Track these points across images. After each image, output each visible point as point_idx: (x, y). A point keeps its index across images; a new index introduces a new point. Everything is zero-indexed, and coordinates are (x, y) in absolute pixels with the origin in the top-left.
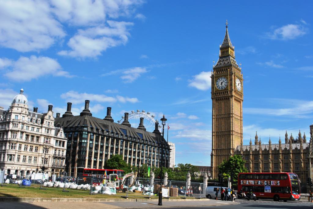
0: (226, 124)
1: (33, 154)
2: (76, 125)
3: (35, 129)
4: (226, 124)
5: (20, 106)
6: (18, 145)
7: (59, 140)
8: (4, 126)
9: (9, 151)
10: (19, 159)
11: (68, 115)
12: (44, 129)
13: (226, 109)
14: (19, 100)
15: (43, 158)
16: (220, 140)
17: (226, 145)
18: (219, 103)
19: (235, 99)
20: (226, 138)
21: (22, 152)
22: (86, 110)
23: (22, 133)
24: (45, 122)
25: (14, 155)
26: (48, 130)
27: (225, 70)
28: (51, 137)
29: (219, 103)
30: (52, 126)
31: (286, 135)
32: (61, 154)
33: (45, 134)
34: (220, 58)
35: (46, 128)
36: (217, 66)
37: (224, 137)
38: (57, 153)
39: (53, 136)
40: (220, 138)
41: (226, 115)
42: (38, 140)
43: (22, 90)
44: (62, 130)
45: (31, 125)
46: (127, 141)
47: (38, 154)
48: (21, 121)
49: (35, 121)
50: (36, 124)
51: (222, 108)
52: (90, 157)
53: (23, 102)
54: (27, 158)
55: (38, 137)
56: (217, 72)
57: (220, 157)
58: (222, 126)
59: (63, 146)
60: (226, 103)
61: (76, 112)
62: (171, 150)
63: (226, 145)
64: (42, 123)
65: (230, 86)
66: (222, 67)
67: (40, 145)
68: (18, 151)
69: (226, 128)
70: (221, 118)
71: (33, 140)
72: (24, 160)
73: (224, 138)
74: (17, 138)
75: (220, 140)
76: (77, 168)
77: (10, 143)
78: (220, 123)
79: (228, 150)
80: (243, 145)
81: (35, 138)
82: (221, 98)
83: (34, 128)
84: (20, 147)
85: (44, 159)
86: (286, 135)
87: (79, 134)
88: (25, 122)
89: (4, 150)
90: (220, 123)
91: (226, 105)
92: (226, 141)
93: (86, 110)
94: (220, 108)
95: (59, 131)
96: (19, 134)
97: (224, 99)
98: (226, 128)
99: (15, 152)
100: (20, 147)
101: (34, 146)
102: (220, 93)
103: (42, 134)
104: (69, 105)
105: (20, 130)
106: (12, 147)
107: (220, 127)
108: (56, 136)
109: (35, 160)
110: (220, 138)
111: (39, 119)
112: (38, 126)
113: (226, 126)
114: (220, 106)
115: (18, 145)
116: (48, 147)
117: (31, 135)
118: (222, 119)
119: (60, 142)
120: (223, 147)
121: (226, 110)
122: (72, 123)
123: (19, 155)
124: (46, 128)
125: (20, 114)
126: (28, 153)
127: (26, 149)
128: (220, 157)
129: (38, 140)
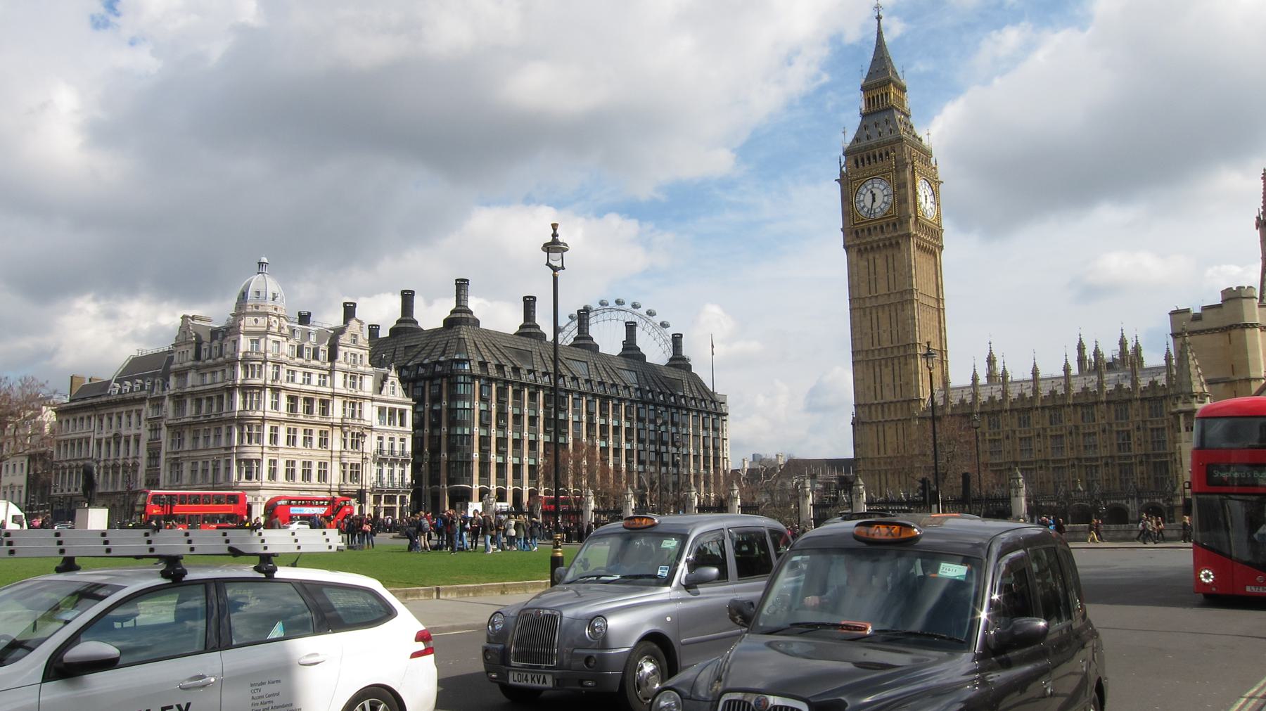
0: (894, 325)
3: (315, 379)
4: (894, 325)
5: (260, 310)
7: (388, 405)
8: (219, 374)
11: (406, 327)
13: (891, 277)
16: (878, 374)
17: (898, 389)
19: (918, 246)
20: (897, 368)
21: (281, 451)
23: (276, 391)
25: (258, 461)
26: (353, 377)
27: (881, 155)
28: (364, 398)
30: (365, 366)
31: (1081, 348)
32: (397, 448)
34: (864, 116)
35: (345, 372)
38: (386, 447)
40: (877, 369)
42: (324, 412)
43: (265, 260)
44: (393, 376)
46: (604, 400)
52: (484, 453)
53: (270, 296)
55: (325, 403)
56: (856, 162)
57: (880, 428)
59: (402, 424)
60: (890, 260)
61: (431, 316)
62: (726, 414)
63: (898, 389)
65: (900, 203)
67: (332, 425)
69: (895, 337)
70: (877, 307)
75: (878, 374)
77: (241, 426)
78: (875, 321)
79: (905, 405)
80: (951, 385)
83: (309, 374)
84: (274, 438)
85: (348, 469)
86: (1081, 348)
87: (445, 385)
88: (284, 358)
89: (226, 449)
90: (875, 321)
91: (891, 265)
92: (897, 379)
94: (872, 277)
95: (385, 377)
97: (885, 245)
98: (895, 337)
100: (274, 438)
101: (316, 430)
102: (869, 230)
104: (407, 298)
106: (250, 436)
107: (876, 335)
108: (376, 396)
109: (323, 475)
110: (877, 369)
113: (894, 332)
115: (267, 427)
117: (302, 396)
119: (392, 411)
120: (889, 396)
123: (275, 461)
124: (345, 372)
126: (300, 453)
127: (291, 440)
128: (880, 428)
129: (324, 412)
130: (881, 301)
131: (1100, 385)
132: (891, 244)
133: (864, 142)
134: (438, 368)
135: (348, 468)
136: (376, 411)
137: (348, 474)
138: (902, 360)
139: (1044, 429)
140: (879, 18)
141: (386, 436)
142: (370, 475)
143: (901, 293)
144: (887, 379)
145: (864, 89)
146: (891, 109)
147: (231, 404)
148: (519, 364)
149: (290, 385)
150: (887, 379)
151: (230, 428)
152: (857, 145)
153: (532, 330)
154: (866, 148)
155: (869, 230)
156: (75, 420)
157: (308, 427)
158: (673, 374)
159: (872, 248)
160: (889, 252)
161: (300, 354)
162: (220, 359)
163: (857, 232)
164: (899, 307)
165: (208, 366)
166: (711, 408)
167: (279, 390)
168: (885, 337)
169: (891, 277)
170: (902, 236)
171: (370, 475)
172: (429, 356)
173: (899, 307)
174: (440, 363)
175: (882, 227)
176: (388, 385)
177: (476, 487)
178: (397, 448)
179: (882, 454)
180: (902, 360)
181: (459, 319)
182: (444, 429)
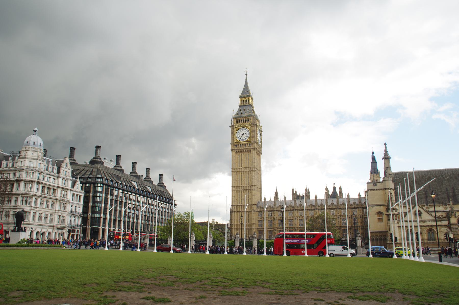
0: (247, 178)
1: (49, 211)
2: (87, 175)
3: (52, 180)
4: (247, 178)
10: (34, 216)
12: (60, 180)
13: (247, 162)
14: (34, 143)
21: (38, 209)
22: (96, 157)
23: (39, 183)
24: (62, 171)
27: (246, 120)
28: (68, 189)
33: (62, 186)
34: (240, 106)
35: (63, 178)
36: (237, 116)
39: (70, 188)
40: (240, 193)
42: (54, 193)
43: (36, 129)
44: (78, 181)
45: (48, 174)
47: (54, 211)
48: (37, 169)
49: (51, 169)
50: (52, 173)
51: (243, 161)
53: (39, 144)
54: (43, 216)
55: (54, 190)
56: (237, 121)
60: (247, 156)
64: (59, 172)
65: (252, 137)
67: (57, 199)
68: (34, 207)
71: (50, 194)
72: (40, 217)
74: (32, 190)
76: (91, 228)
77: (23, 197)
81: (52, 191)
83: (50, 178)
84: (36, 202)
88: (42, 170)
89: (14, 206)
93: (96, 157)
94: (240, 161)
96: (35, 185)
99: (30, 208)
100: (36, 202)
101: (51, 201)
102: (241, 145)
103: (59, 186)
105: (36, 180)
106: (26, 201)
108: (72, 189)
109: (51, 219)
110: (240, 193)
111: (56, 167)
114: (240, 159)
115: (34, 198)
116: (65, 202)
117: (53, 188)
119: (77, 195)
121: (247, 163)
122: (80, 173)
124: (63, 178)
125: (37, 159)
126: (45, 210)
127: (42, 204)
129: (54, 193)
130: (243, 170)
134: (89, 180)
135: (61, 218)
136: (72, 195)
138: (250, 191)
140: (246, 75)
141: (74, 205)
145: (241, 97)
146: (250, 105)
147: (18, 188)
148: (117, 181)
149: (43, 182)
151: (17, 198)
153: (120, 168)
155: (241, 145)
158: (162, 189)
160: (247, 153)
161: (47, 170)
162: (12, 168)
163: (236, 145)
164: (249, 172)
165: (5, 171)
167: (40, 183)
169: (247, 162)
172: (84, 174)
173: (249, 172)
174: (90, 178)
175: (245, 145)
176: (76, 185)
177: (101, 228)
178: (77, 211)
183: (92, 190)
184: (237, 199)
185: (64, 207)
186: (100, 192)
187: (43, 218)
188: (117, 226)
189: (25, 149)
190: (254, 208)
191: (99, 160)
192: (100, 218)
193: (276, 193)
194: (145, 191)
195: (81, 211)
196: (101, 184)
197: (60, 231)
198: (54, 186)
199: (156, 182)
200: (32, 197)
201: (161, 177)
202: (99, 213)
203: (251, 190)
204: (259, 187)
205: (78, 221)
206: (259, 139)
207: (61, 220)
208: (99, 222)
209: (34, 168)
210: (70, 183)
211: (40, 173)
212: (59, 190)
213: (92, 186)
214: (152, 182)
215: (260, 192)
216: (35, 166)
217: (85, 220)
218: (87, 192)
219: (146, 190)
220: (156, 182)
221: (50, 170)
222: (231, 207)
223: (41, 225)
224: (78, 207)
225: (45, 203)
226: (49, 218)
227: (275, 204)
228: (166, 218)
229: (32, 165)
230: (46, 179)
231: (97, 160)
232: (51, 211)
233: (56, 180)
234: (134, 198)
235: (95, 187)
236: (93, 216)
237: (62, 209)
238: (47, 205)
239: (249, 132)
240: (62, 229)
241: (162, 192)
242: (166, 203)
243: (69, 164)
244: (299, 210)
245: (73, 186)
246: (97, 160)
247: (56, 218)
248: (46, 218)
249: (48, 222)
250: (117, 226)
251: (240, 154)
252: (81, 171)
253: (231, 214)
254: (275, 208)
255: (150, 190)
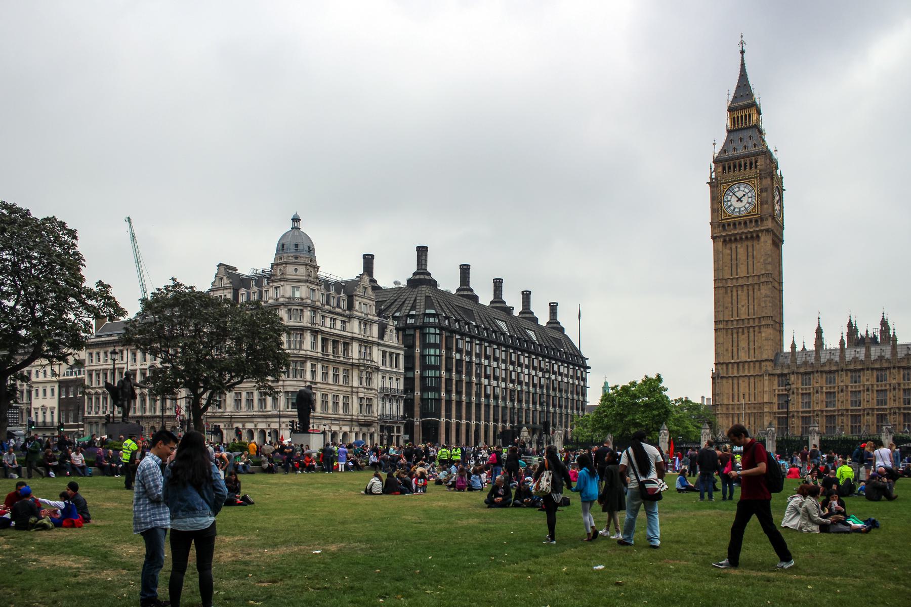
1: (340, 388)
2: (406, 310)
3: (338, 323)
6: (308, 365)
7: (388, 350)
9: (287, 383)
13: (750, 263)
15: (361, 398)
17: (752, 352)
18: (731, 249)
21: (319, 386)
23: (315, 332)
24: (356, 304)
28: (373, 343)
29: (731, 249)
33: (360, 337)
35: (360, 320)
37: (746, 331)
39: (376, 340)
40: (735, 336)
41: (750, 279)
42: (346, 350)
48: (309, 301)
49: (335, 301)
50: (338, 310)
55: (346, 345)
58: (740, 306)
60: (750, 249)
63: (752, 352)
64: (350, 307)
66: (739, 158)
67: (353, 365)
69: (751, 311)
71: (337, 353)
73: (746, 335)
78: (734, 298)
81: (341, 347)
82: (749, 236)
83: (335, 320)
84: (313, 372)
85: (364, 402)
88: (319, 304)
90: (734, 298)
91: (750, 254)
92: (751, 344)
94: (734, 262)
96: (308, 337)
97: (747, 238)
98: (751, 311)
100: (313, 372)
104: (368, 260)
105: (309, 325)
107: (735, 308)
109: (346, 405)
110: (735, 336)
112: (344, 316)
114: (734, 256)
115: (308, 365)
116: (369, 370)
118: (740, 288)
119: (391, 354)
120: (743, 357)
129: (346, 350)
130: (740, 282)
131: (868, 355)
132: (752, 237)
133: (731, 154)
134: (410, 321)
136: (380, 353)
137: (364, 407)
138: (756, 329)
139: (872, 385)
142: (377, 409)
143: (759, 276)
144: (743, 344)
149: (323, 328)
150: (743, 344)
152: (725, 156)
153: (470, 293)
154: (732, 159)
156: (106, 353)
157: (336, 366)
158: (557, 335)
159: (736, 240)
160: (750, 243)
161: (328, 303)
164: (756, 287)
166: (576, 361)
168: (743, 310)
169: (750, 263)
170: (762, 231)
171: (377, 409)
174: (412, 317)
179: (736, 402)
180: (756, 329)
181: (422, 279)
182: (418, 372)
183: (418, 343)
184: (727, 350)
185: (369, 379)
186: (435, 346)
187: (331, 404)
188: (474, 417)
189: (294, 260)
190: (770, 369)
191: (426, 277)
192: (439, 400)
193: (819, 332)
194: (525, 341)
195: (402, 387)
196: (435, 328)
197: (365, 429)
198: (345, 337)
199: (543, 320)
200: (304, 362)
201: (553, 308)
202: (437, 389)
203: (760, 327)
204: (777, 320)
205: (396, 409)
206: (777, 207)
207: (364, 407)
208: (439, 409)
209: (302, 299)
210: (375, 329)
211: (315, 309)
212: (356, 345)
213: (418, 335)
214: (535, 320)
215: (781, 332)
216: (304, 296)
217: (409, 406)
218: (409, 347)
219: (527, 338)
220: (543, 320)
221: (333, 302)
222: (713, 367)
223: (327, 419)
224: (394, 378)
225: (331, 373)
226: (341, 404)
227: (818, 357)
228: (570, 396)
229: (297, 295)
230: (328, 322)
231: (422, 277)
232: (344, 389)
233: (348, 324)
234: (503, 356)
235: (424, 335)
236: (425, 396)
237: (364, 384)
238: (336, 376)
239: (754, 193)
240: (368, 424)
241: (558, 341)
242: (568, 363)
243: (370, 289)
244: (877, 369)
245: (382, 335)
246: (422, 277)
247: (355, 403)
248: (336, 404)
249: (341, 412)
250: (474, 417)
251: (734, 246)
252: (392, 304)
253: (713, 383)
254: (818, 366)
255: (535, 339)
